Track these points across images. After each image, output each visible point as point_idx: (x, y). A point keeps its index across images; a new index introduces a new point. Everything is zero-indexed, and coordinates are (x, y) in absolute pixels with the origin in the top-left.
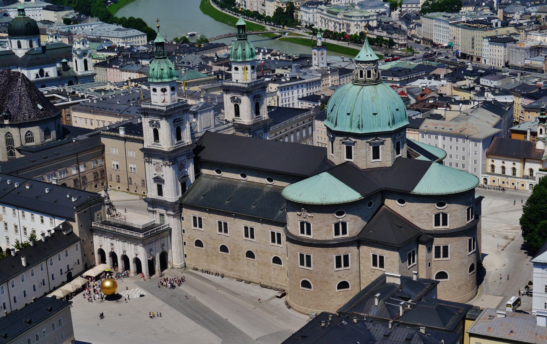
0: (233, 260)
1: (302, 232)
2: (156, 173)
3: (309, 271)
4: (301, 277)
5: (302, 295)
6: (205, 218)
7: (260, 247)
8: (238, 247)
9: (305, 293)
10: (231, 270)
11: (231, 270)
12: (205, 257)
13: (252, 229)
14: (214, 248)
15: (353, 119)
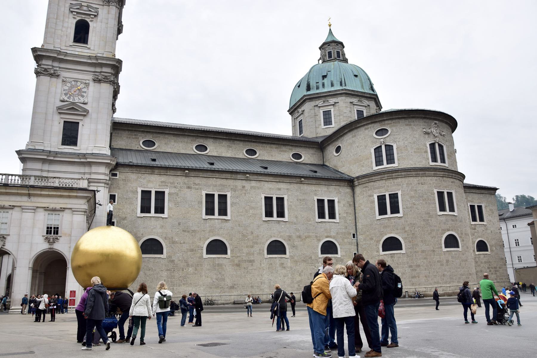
0: (238, 265)
1: (434, 159)
2: (66, 99)
3: (453, 218)
4: (444, 231)
5: (447, 261)
6: (173, 190)
7: (297, 230)
8: (250, 237)
9: (452, 257)
10: (232, 287)
11: (232, 287)
12: (165, 274)
13: (280, 200)
14: (192, 250)
15: (363, 81)
